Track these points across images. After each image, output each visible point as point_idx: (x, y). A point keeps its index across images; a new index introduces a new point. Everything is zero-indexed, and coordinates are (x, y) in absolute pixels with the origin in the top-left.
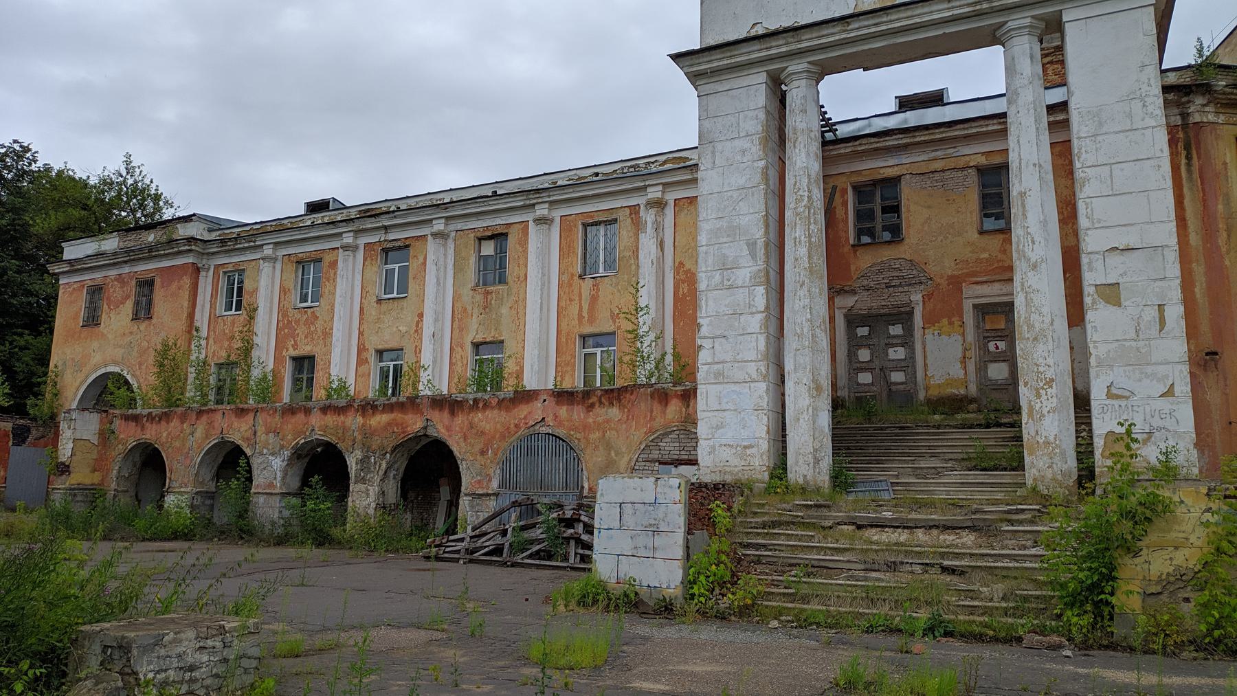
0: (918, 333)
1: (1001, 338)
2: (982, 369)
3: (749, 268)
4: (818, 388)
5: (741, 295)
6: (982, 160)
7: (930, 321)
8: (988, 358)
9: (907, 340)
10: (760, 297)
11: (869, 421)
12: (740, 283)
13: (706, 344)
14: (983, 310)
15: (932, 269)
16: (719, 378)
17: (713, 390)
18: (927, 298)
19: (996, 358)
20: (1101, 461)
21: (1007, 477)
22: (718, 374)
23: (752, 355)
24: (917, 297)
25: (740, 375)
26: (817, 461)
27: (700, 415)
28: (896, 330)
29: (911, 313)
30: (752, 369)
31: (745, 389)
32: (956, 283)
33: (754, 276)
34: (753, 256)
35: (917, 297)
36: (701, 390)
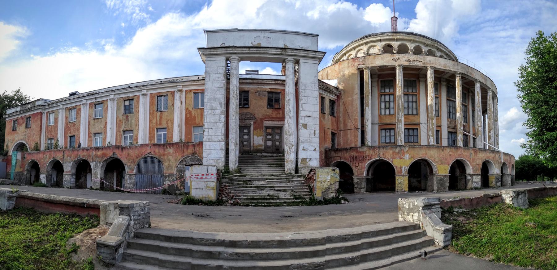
0: (252, 132)
1: (270, 135)
2: (265, 142)
3: (220, 110)
4: (237, 144)
5: (217, 117)
6: (269, 90)
7: (255, 129)
8: (266, 140)
9: (249, 134)
10: (223, 118)
11: (247, 155)
12: (217, 113)
13: (206, 130)
14: (267, 127)
15: (256, 116)
16: (210, 140)
17: (208, 143)
18: (255, 123)
19: (269, 140)
20: (300, 165)
21: (278, 169)
22: (209, 139)
23: (220, 134)
24: (252, 123)
25: (216, 140)
26: (236, 164)
27: (204, 150)
28: (246, 131)
29: (250, 127)
30: (220, 138)
31: (218, 143)
32: (262, 120)
33: (221, 112)
34: (221, 106)
35: (252, 123)
36: (204, 143)
